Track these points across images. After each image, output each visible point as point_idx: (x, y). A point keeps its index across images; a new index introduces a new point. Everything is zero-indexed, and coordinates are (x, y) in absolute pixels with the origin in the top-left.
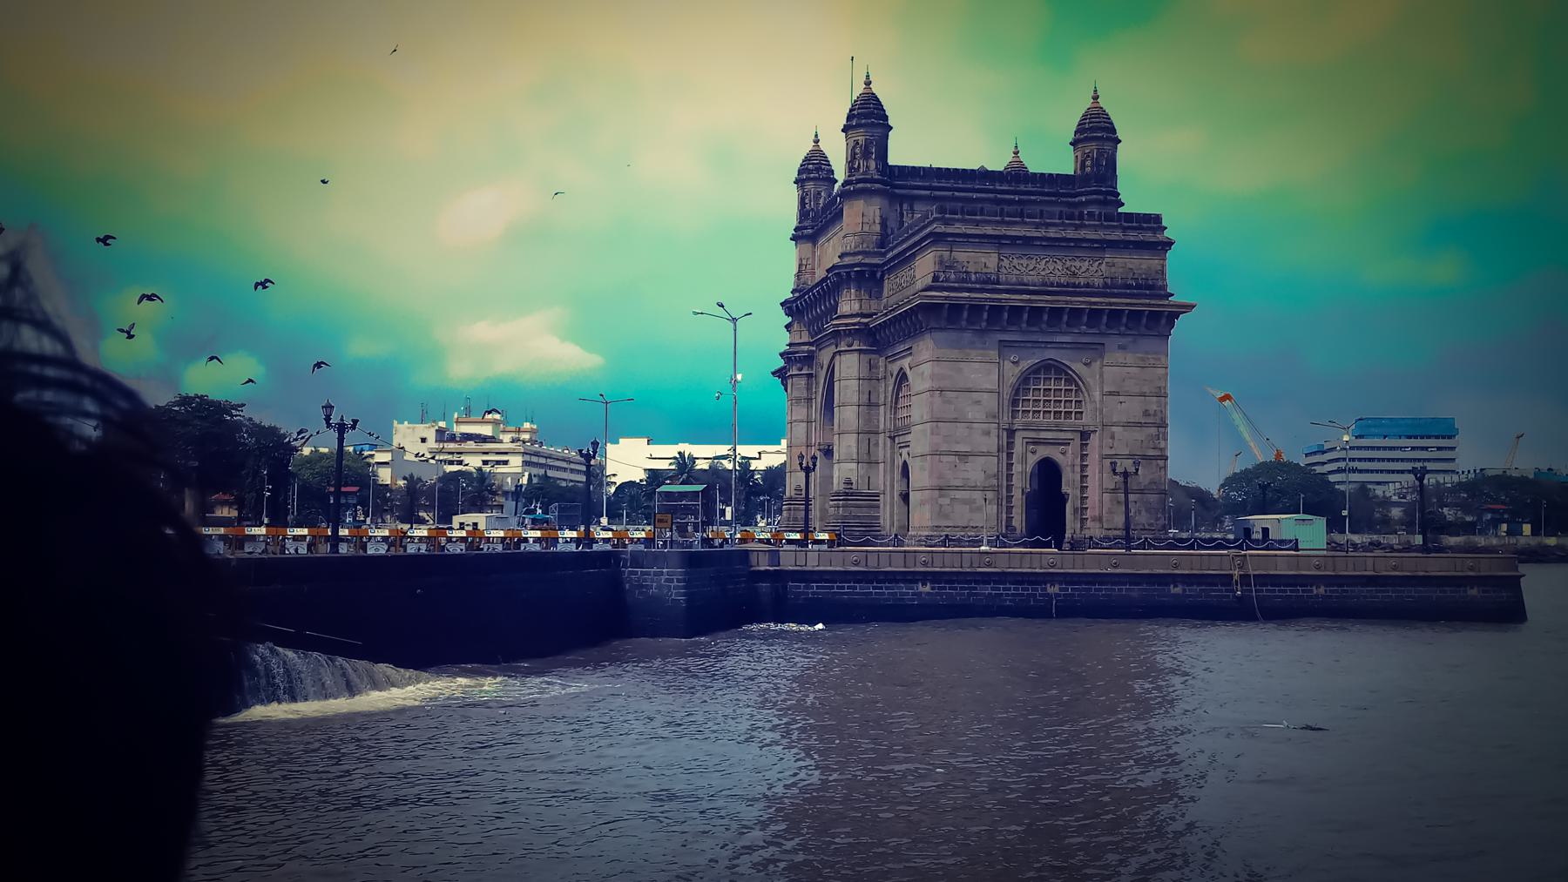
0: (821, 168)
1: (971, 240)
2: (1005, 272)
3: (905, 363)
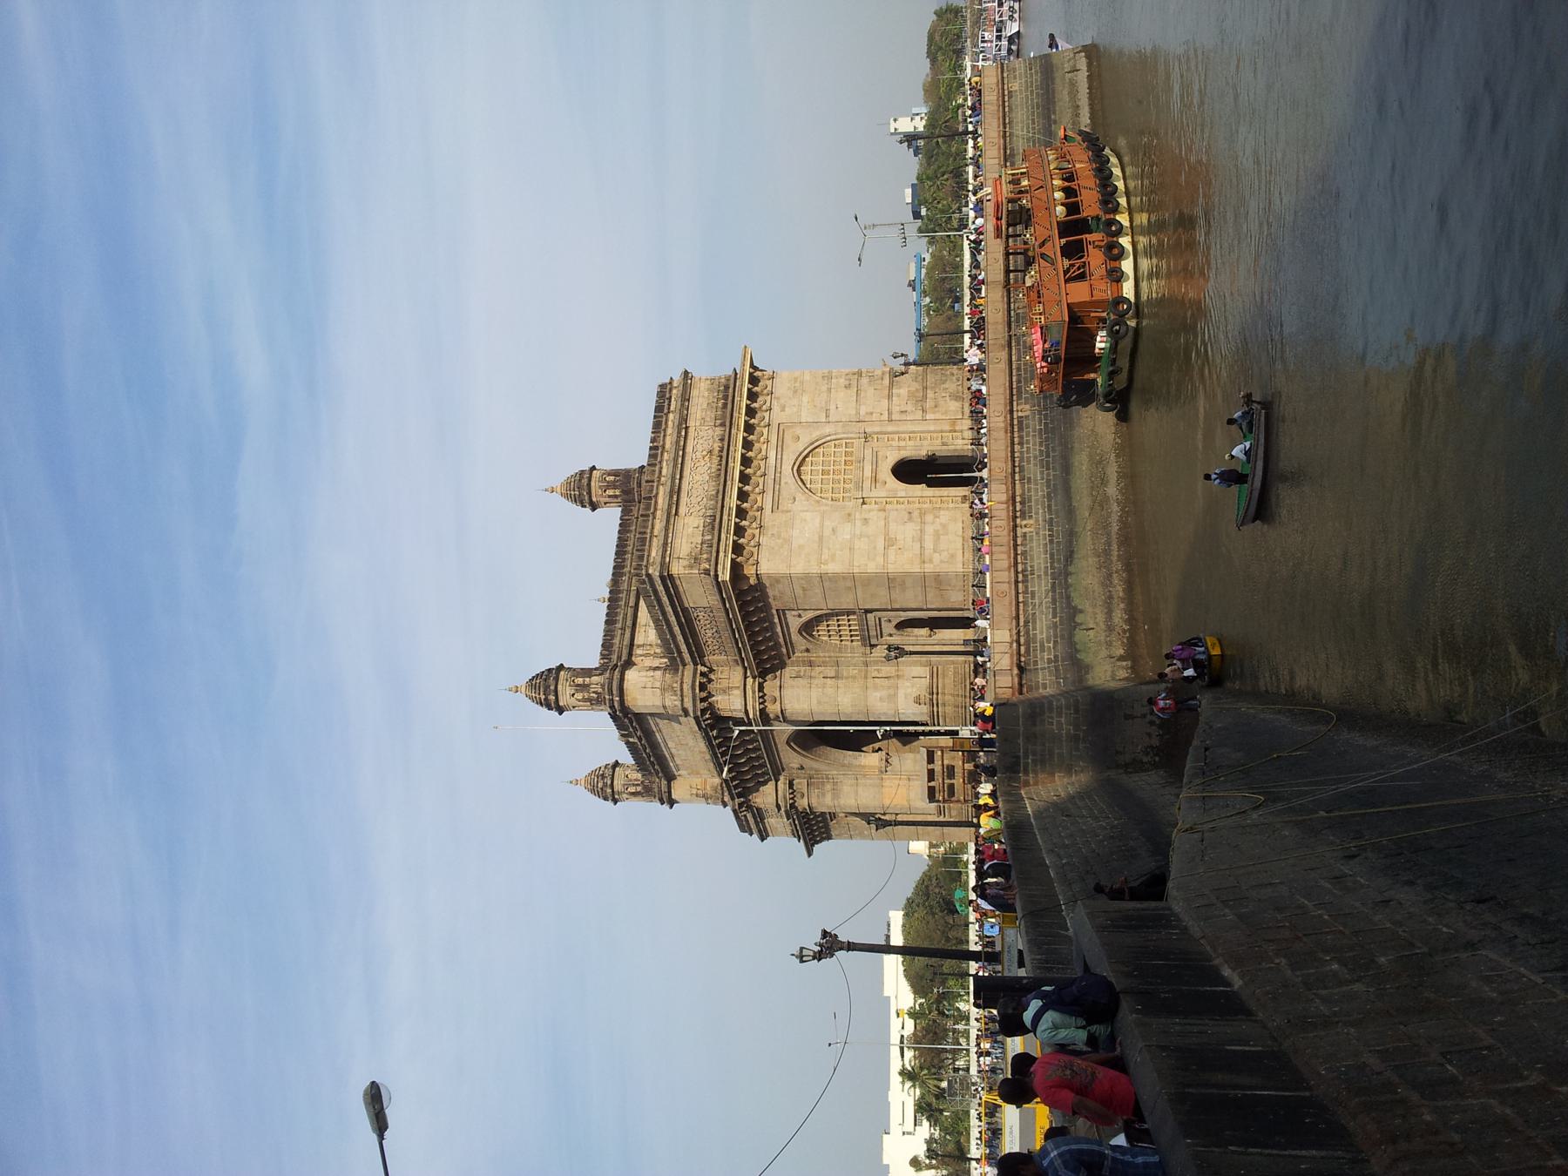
1: (670, 541)
2: (704, 510)
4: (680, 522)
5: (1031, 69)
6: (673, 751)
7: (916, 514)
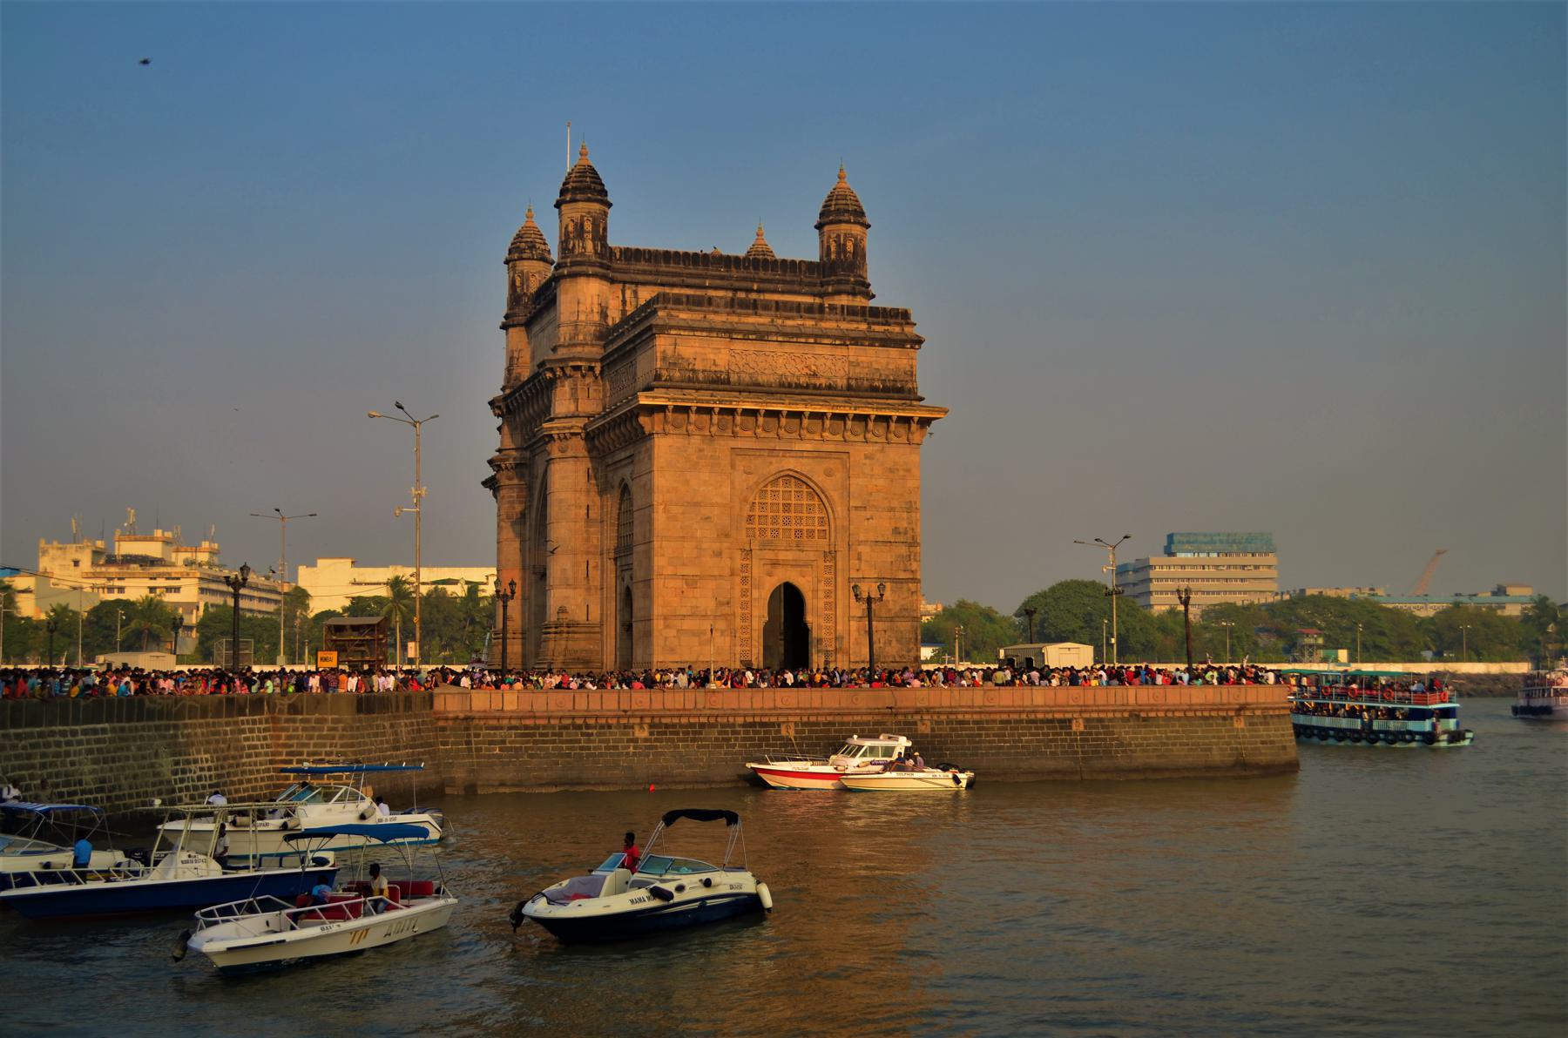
0: (534, 247)
1: (697, 333)
2: (737, 370)
3: (626, 472)
4: (719, 343)
5: (1262, 743)
6: (546, 332)
7: (726, 610)
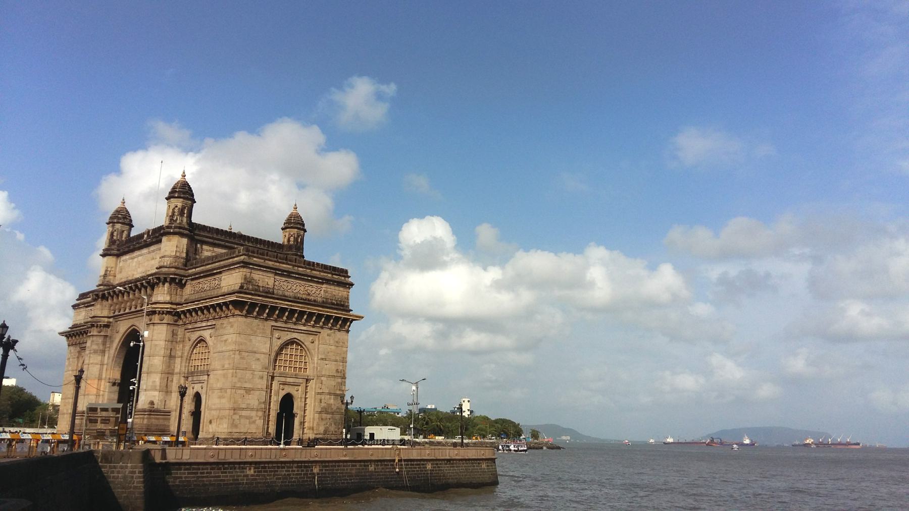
1: (262, 268)
3: (206, 334)
